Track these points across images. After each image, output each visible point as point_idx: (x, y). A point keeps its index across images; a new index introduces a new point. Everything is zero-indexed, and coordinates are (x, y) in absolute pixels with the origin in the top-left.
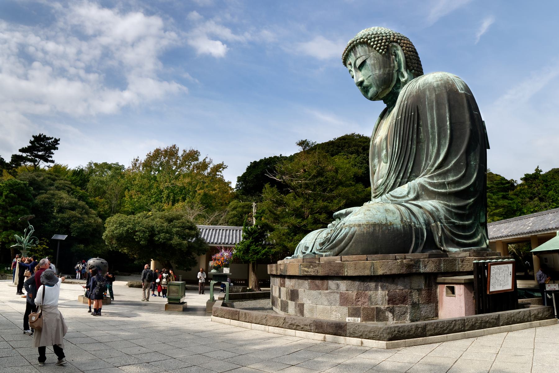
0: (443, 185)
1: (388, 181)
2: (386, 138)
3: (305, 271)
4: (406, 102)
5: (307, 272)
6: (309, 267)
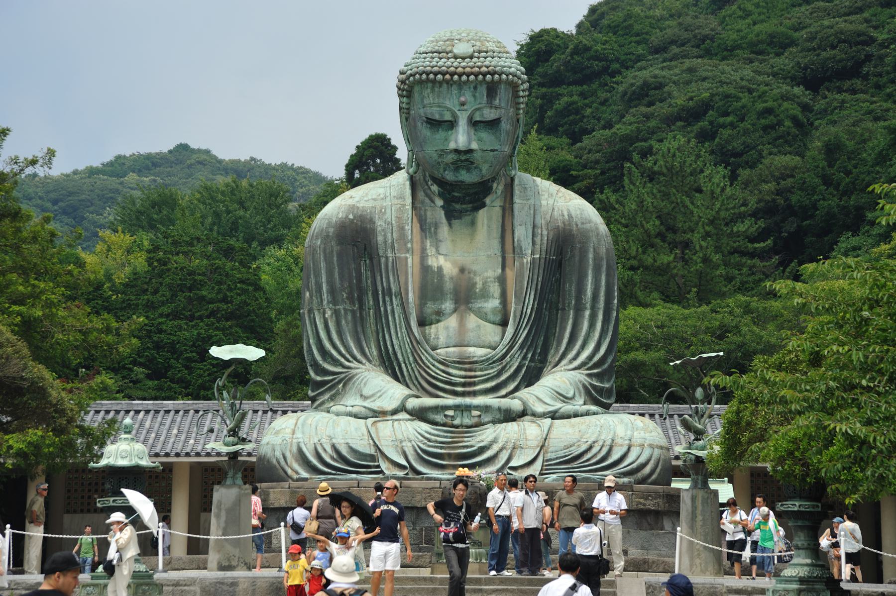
0: (600, 391)
1: (508, 358)
2: (502, 280)
3: (641, 503)
4: (545, 233)
5: (644, 505)
6: (646, 499)
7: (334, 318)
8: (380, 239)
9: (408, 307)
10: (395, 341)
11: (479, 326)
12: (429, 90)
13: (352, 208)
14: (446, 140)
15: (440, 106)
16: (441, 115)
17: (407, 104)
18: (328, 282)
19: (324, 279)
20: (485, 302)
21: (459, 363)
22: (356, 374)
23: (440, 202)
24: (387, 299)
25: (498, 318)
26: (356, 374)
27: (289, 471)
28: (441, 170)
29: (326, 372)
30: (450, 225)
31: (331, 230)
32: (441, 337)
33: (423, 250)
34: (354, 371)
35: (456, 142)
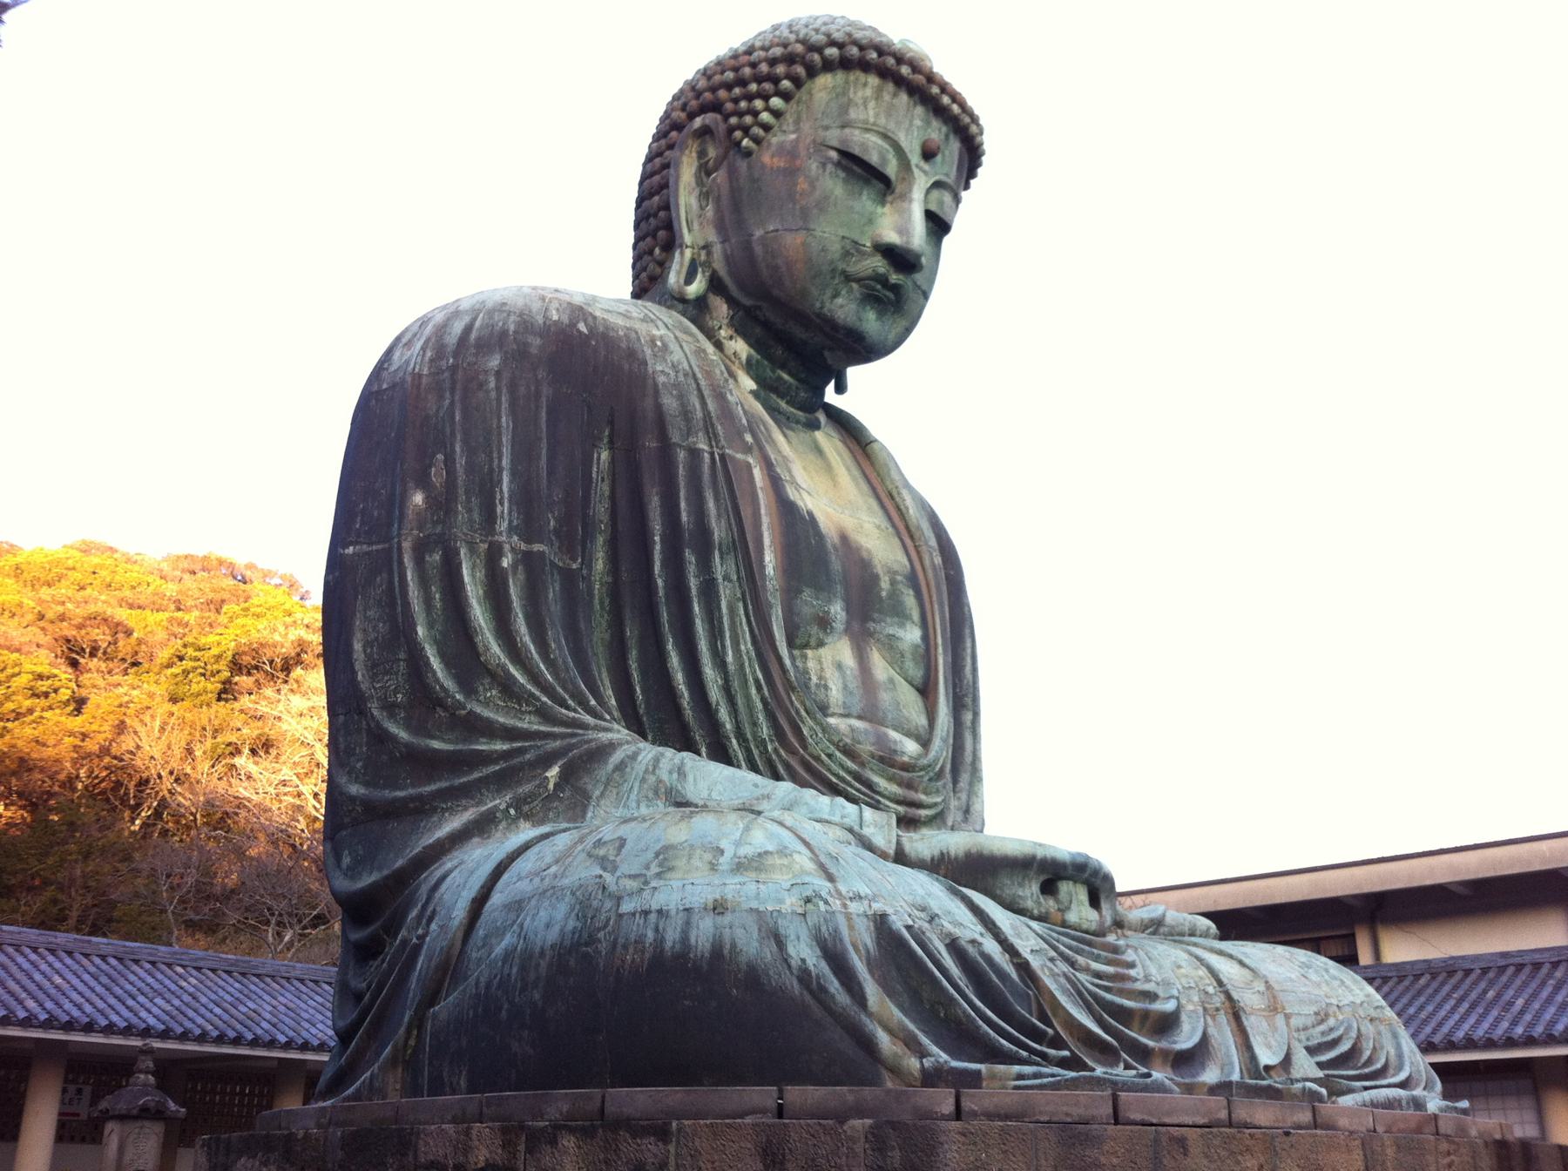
7: (521, 576)
8: (670, 403)
9: (764, 586)
10: (709, 672)
11: (891, 680)
12: (869, 92)
13: (578, 312)
14: (870, 221)
15: (885, 137)
16: (884, 160)
17: (777, 114)
18: (514, 474)
19: (505, 462)
20: (902, 625)
21: (882, 760)
22: (611, 747)
23: (749, 384)
24: (690, 557)
25: (917, 673)
26: (611, 747)
27: (884, 1039)
28: (829, 293)
29: (477, 727)
30: (785, 436)
31: (535, 342)
32: (831, 684)
33: (768, 466)
34: (592, 735)
35: (903, 231)
